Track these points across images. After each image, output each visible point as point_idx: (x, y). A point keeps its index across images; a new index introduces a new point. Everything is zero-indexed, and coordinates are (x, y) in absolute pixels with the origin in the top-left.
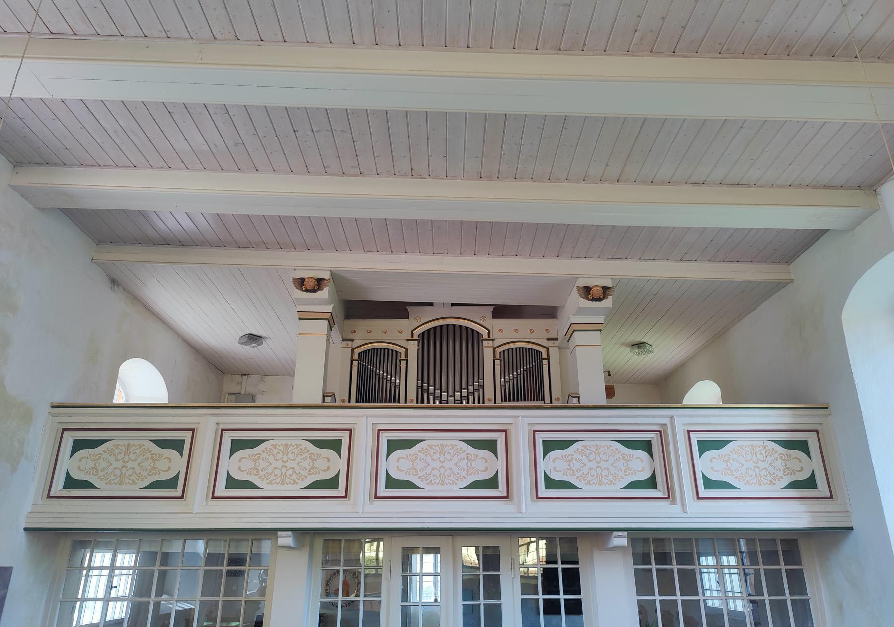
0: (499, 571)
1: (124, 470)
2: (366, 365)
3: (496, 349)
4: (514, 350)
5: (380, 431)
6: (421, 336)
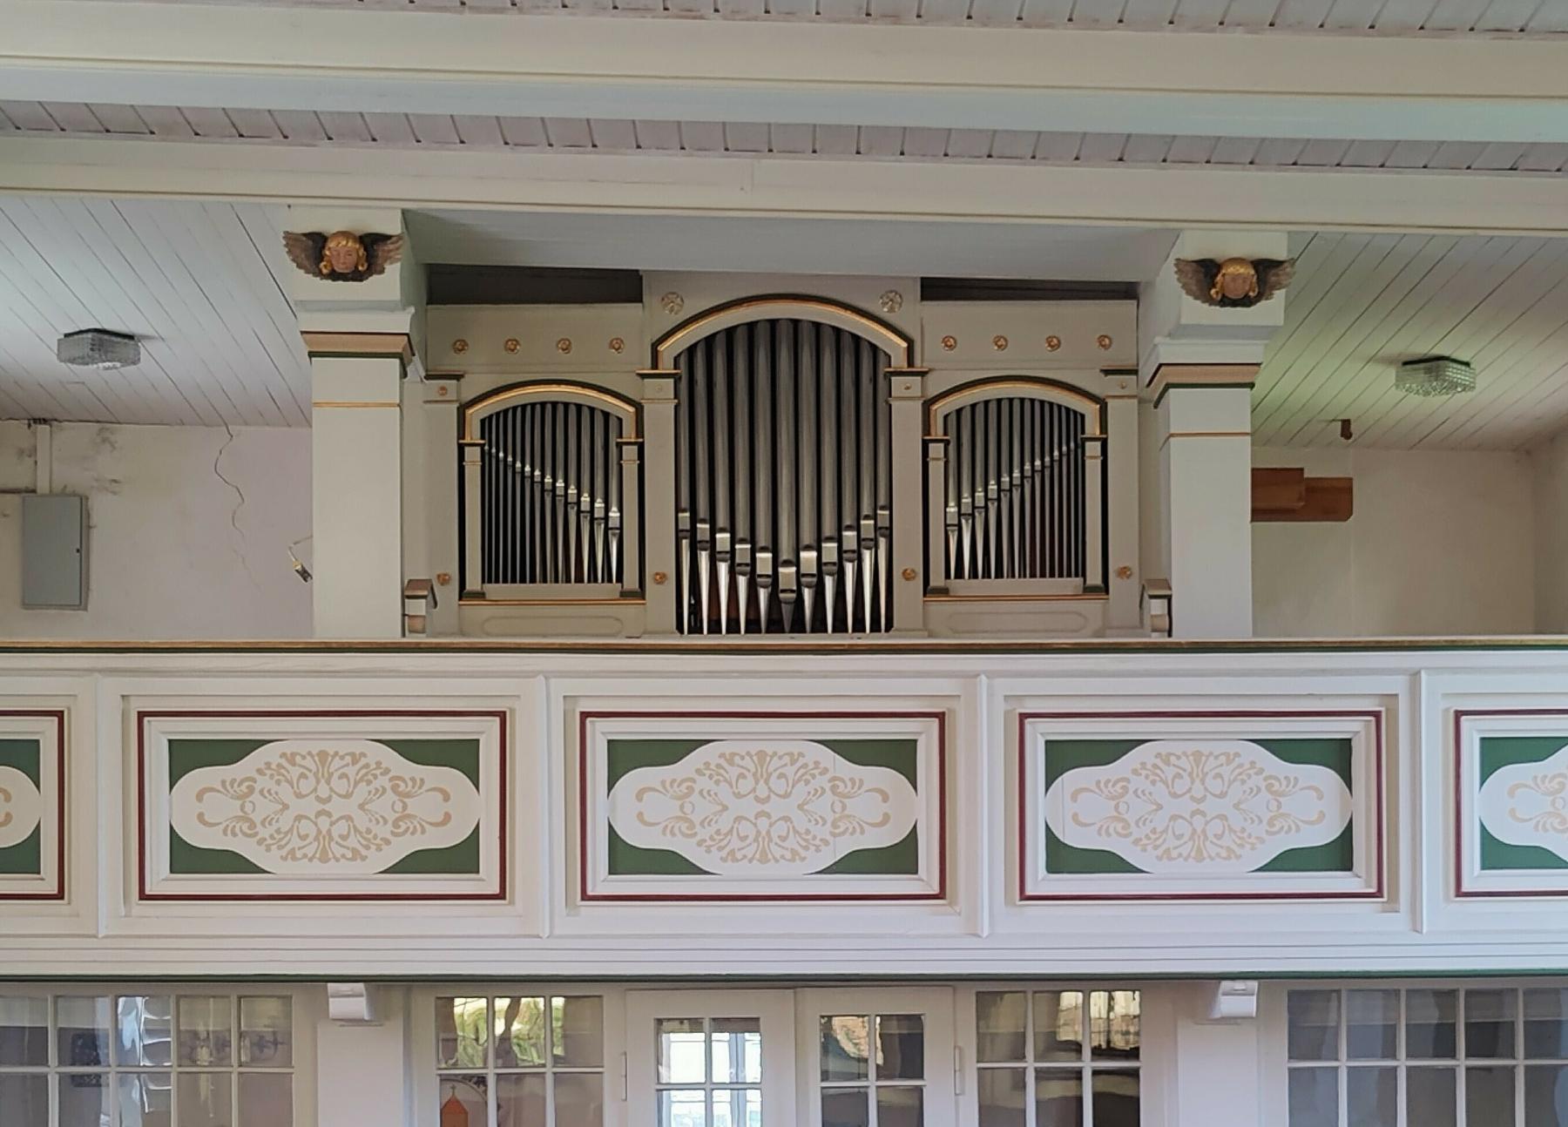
0: (921, 1077)
2: (510, 459)
3: (935, 407)
4: (993, 407)
6: (683, 361)
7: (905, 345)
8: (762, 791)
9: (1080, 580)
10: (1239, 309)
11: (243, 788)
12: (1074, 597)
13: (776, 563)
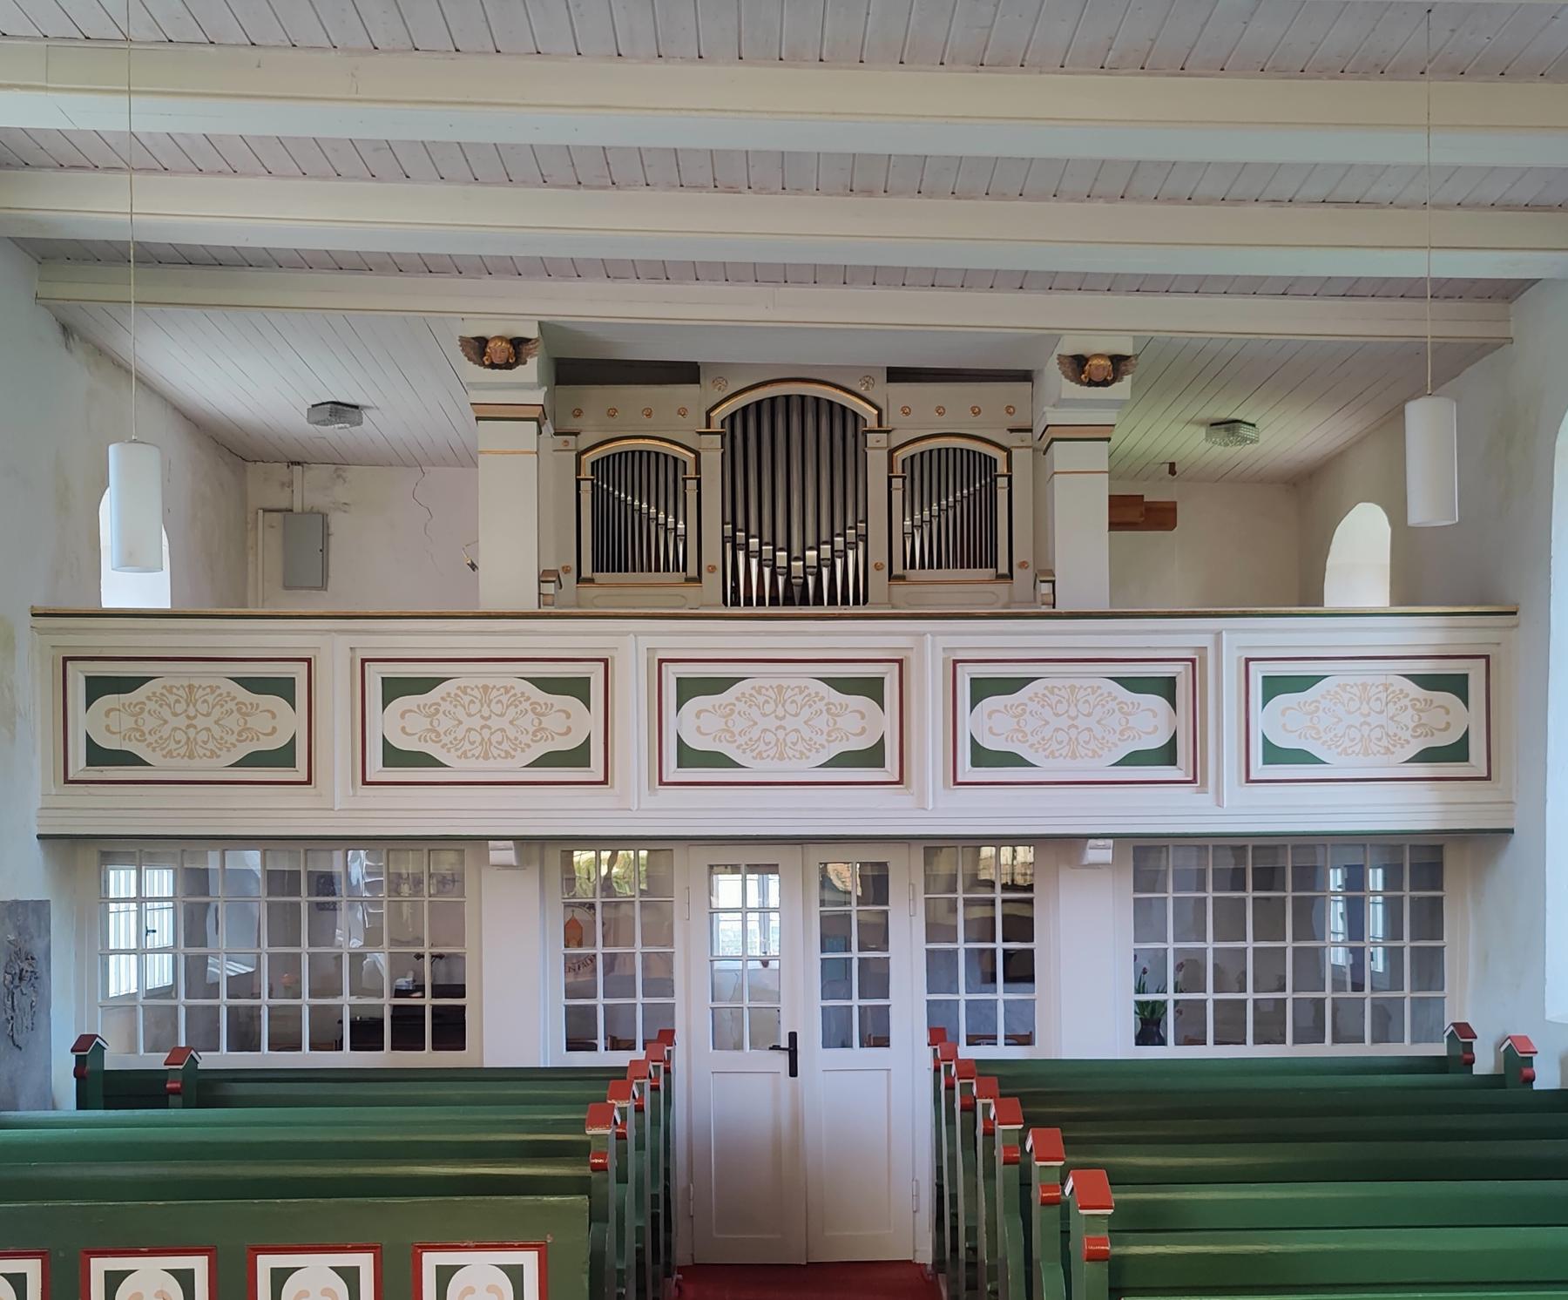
1: (192, 732)
2: (611, 489)
3: (896, 454)
4: (935, 454)
5: (661, 661)
6: (727, 423)
7: (876, 412)
8: (780, 712)
9: (993, 570)
10: (1100, 388)
11: (432, 709)
12: (989, 582)
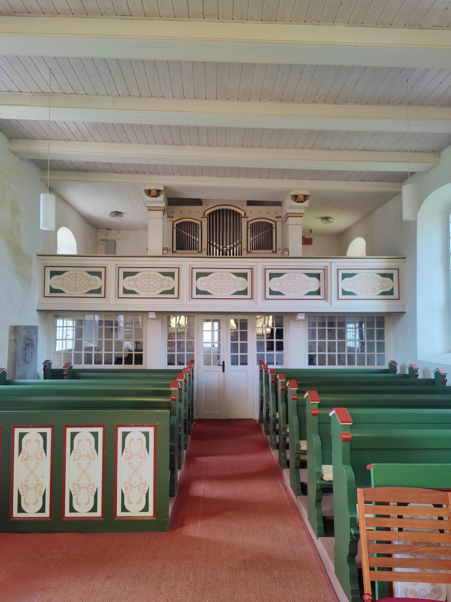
0: (247, 329)
1: (76, 285)
4: (258, 223)
5: (192, 268)
9: (272, 251)
13: (223, 247)
